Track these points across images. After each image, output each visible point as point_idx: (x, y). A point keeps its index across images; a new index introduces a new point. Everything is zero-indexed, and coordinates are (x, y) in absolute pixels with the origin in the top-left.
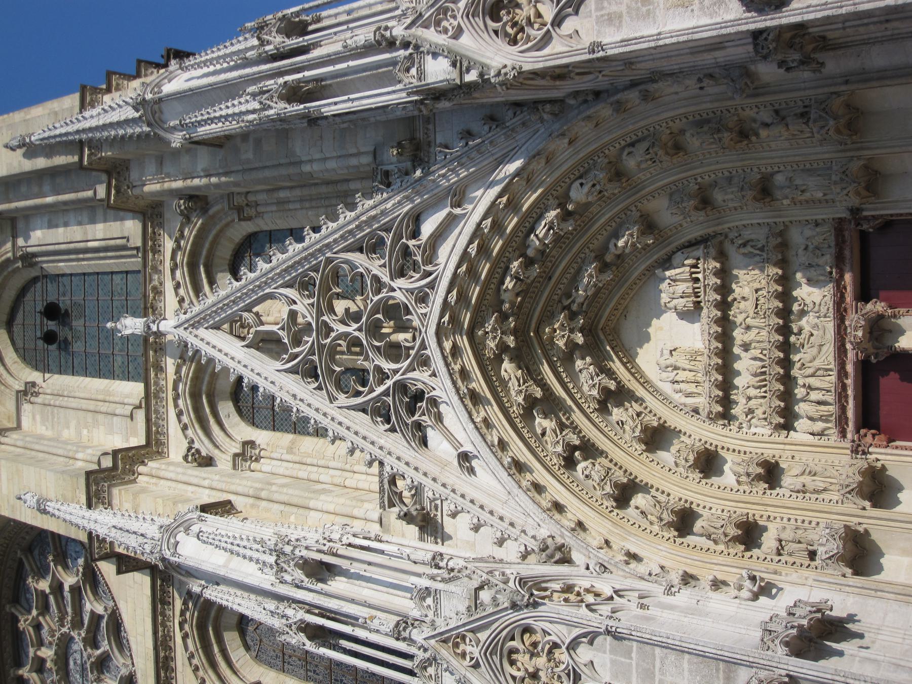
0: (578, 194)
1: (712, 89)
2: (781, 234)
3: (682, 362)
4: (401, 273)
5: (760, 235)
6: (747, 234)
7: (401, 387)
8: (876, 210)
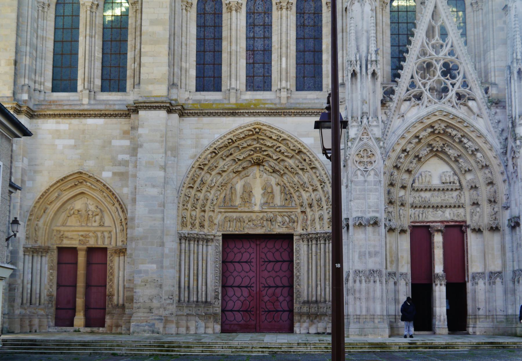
0: (479, 155)
1: (504, 198)
2: (462, 206)
3: (427, 179)
4: (457, 94)
5: (462, 201)
6: (463, 197)
7: (421, 93)
8: (469, 231)
